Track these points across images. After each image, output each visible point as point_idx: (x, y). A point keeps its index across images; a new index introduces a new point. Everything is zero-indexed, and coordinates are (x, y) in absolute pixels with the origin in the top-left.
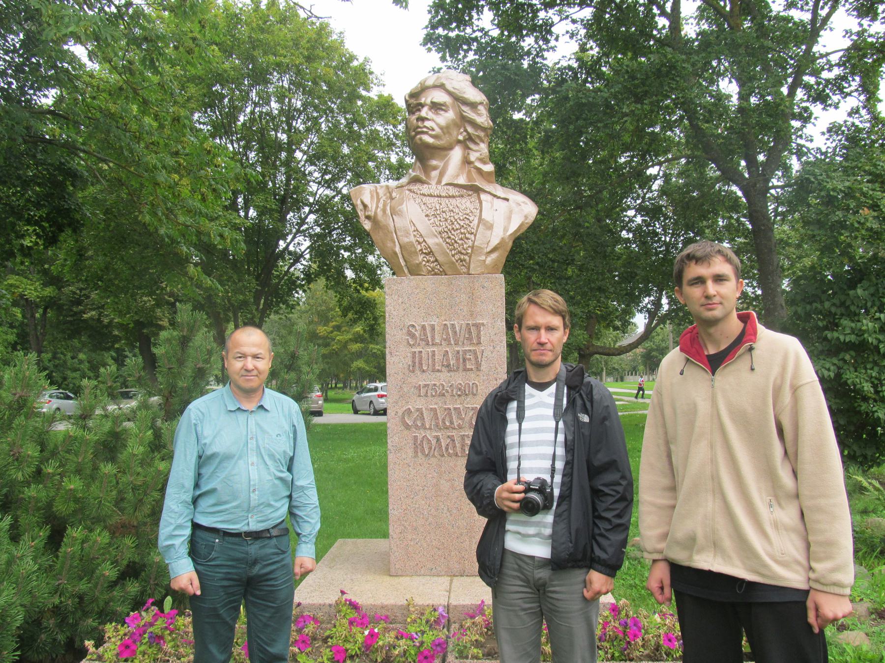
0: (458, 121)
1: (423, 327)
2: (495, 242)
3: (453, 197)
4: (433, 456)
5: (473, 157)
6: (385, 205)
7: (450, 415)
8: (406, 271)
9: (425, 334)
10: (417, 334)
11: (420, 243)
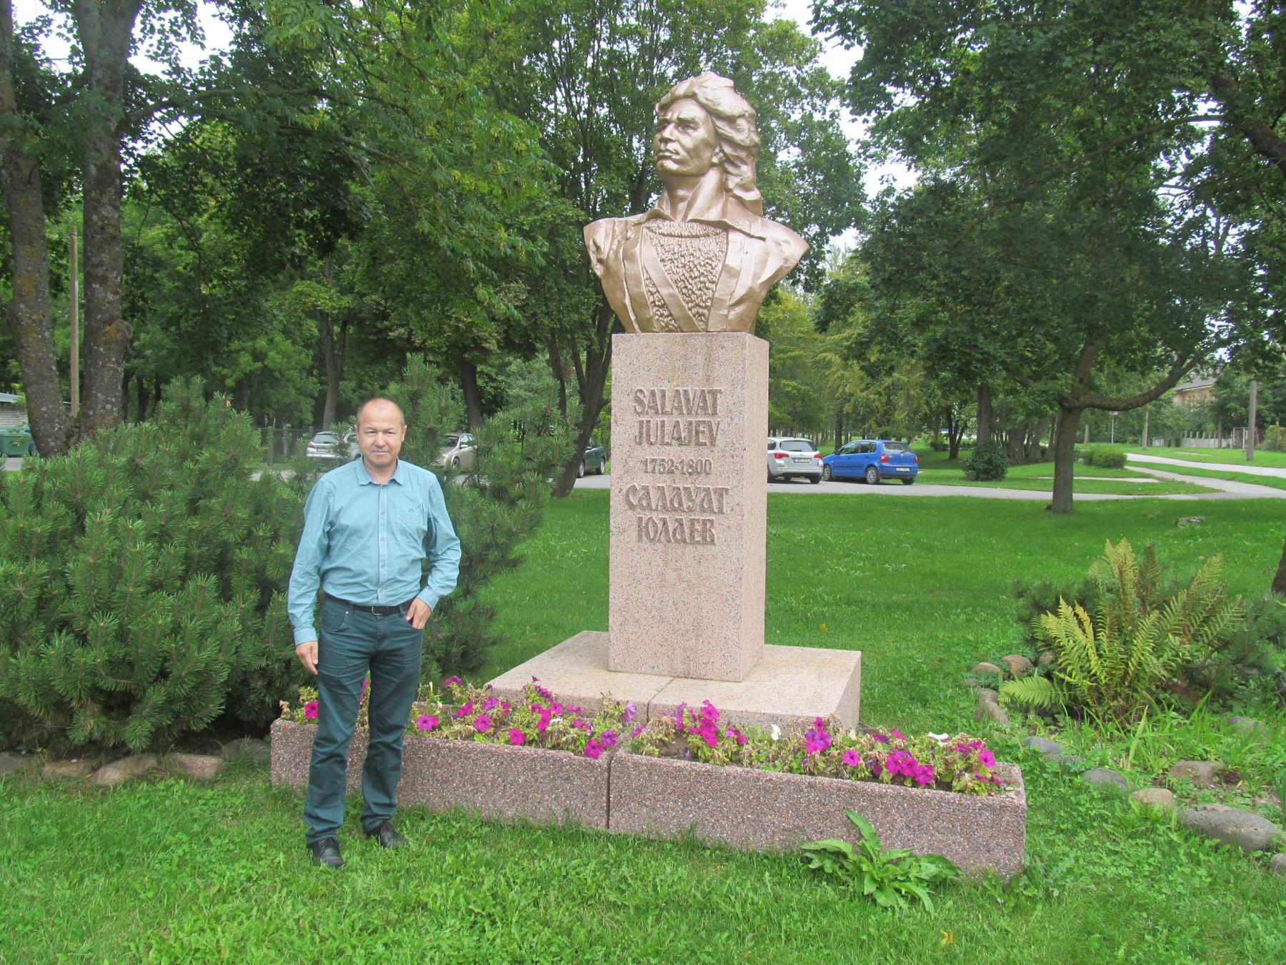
0: (712, 140)
1: (653, 393)
2: (740, 292)
3: (697, 237)
4: (659, 541)
6: (618, 247)
7: (679, 494)
8: (636, 326)
9: (655, 402)
11: (652, 294)
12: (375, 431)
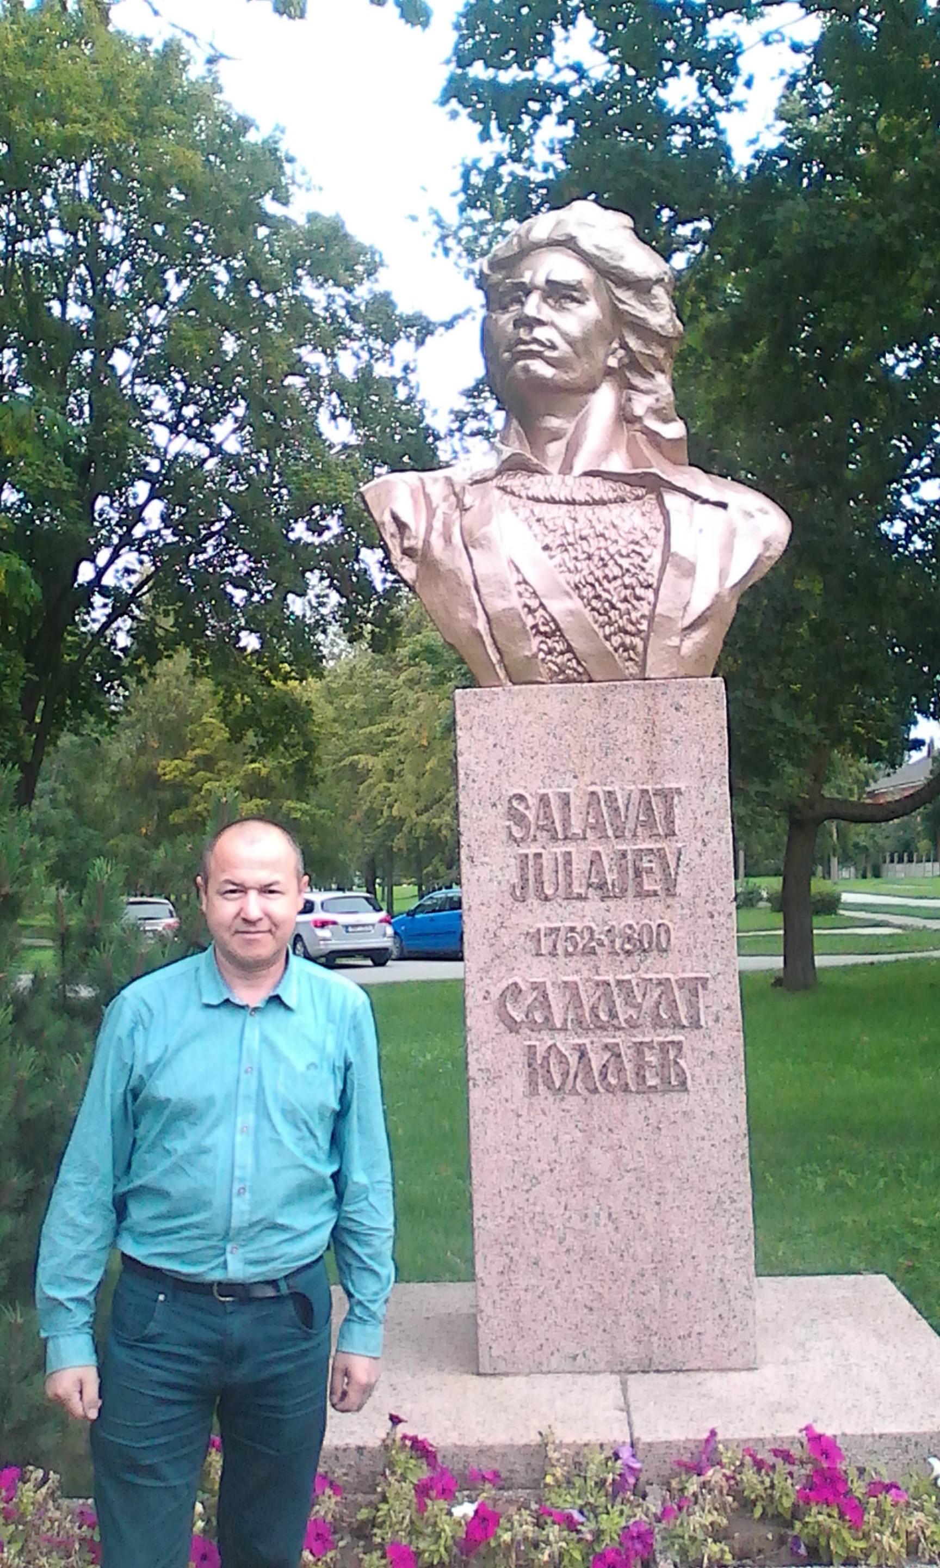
0: (608, 324)
1: (544, 799)
2: (700, 604)
3: (603, 503)
5: (640, 404)
6: (447, 526)
7: (608, 996)
8: (502, 674)
10: (531, 815)
11: (531, 611)
12: (241, 889)
